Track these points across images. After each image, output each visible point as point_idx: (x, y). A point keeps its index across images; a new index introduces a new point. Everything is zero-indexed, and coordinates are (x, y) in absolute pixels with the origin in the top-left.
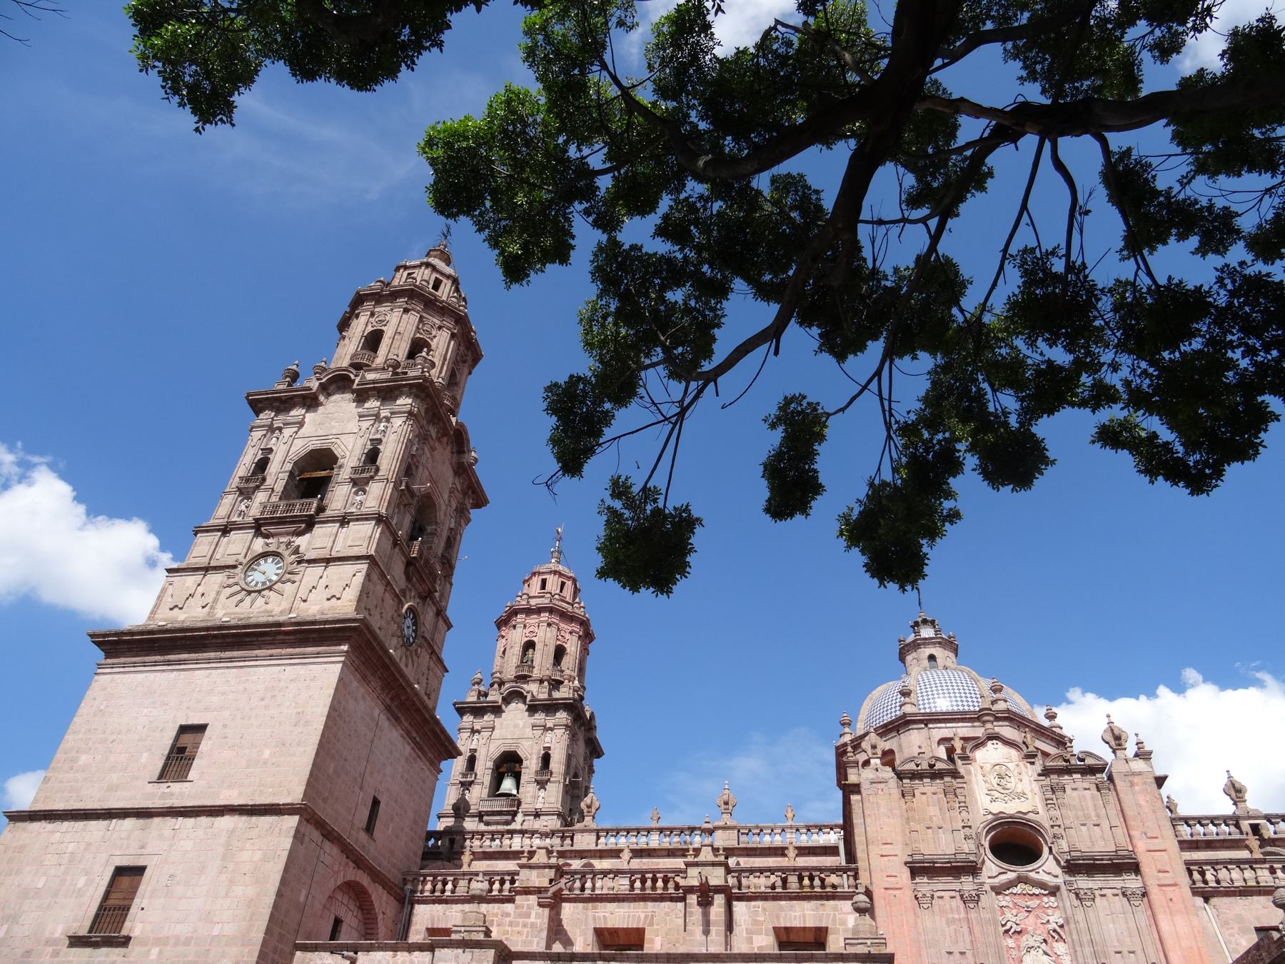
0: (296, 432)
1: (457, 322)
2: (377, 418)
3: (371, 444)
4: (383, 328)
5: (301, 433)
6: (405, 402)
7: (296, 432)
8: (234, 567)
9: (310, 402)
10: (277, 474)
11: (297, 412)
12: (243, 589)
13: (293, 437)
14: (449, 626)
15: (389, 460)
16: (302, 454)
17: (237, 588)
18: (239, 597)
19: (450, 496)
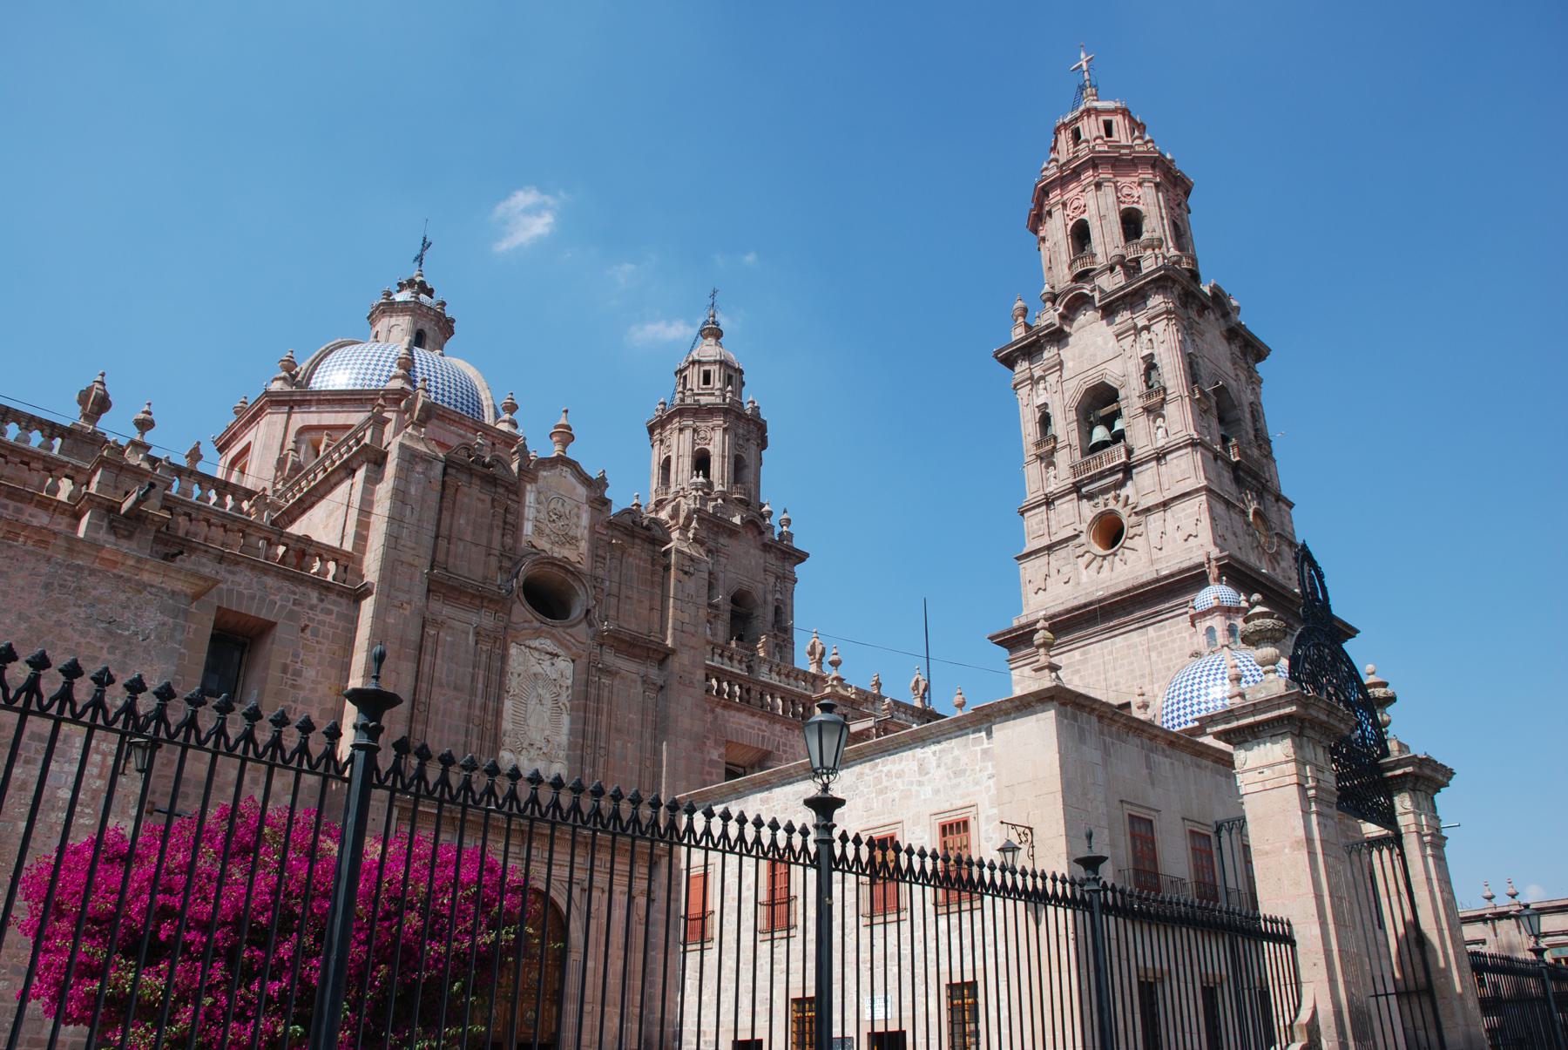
0: (1061, 376)
1: (1153, 167)
2: (1138, 331)
3: (1145, 362)
4: (1083, 216)
5: (1066, 375)
6: (1157, 301)
7: (1061, 376)
8: (1077, 536)
9: (1058, 337)
10: (1064, 427)
11: (1049, 353)
12: (1096, 556)
13: (1061, 381)
14: (1291, 505)
15: (1172, 373)
16: (1079, 397)
17: (1088, 557)
18: (1095, 565)
19: (1235, 369)
